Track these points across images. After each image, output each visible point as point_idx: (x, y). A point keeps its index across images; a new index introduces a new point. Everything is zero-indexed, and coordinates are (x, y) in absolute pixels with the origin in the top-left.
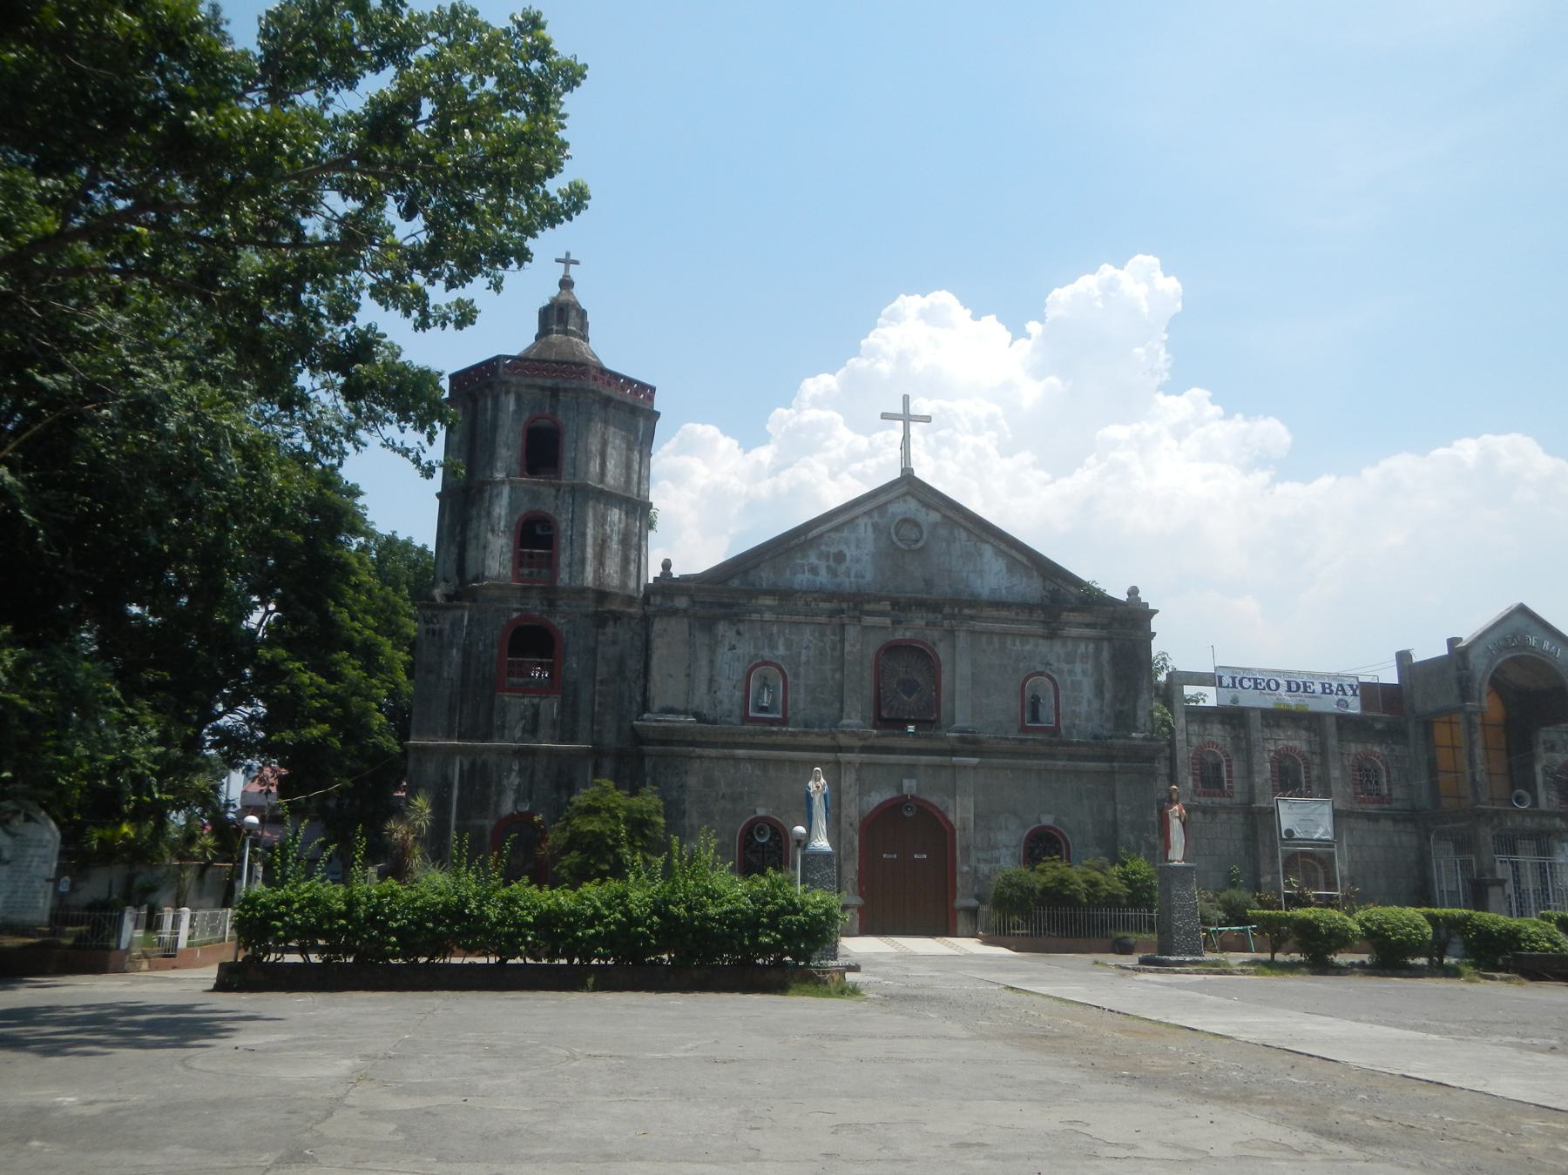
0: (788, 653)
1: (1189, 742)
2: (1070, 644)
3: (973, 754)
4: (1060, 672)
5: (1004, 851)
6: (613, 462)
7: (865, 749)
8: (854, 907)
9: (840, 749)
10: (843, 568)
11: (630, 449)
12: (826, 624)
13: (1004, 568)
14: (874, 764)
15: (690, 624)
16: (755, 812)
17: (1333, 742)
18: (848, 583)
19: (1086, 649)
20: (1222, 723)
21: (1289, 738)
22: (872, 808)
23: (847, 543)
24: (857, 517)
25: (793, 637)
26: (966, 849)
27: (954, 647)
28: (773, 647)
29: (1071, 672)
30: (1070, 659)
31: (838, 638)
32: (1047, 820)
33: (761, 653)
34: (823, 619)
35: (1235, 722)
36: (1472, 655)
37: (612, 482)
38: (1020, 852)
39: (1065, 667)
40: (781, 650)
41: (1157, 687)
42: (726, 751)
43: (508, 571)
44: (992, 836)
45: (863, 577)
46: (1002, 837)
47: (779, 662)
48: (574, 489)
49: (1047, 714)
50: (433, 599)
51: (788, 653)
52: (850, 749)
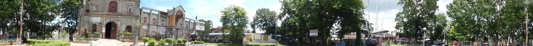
3: (121, 15)
7: (106, 15)
9: (104, 15)
41: (140, 9)
46: (123, 26)
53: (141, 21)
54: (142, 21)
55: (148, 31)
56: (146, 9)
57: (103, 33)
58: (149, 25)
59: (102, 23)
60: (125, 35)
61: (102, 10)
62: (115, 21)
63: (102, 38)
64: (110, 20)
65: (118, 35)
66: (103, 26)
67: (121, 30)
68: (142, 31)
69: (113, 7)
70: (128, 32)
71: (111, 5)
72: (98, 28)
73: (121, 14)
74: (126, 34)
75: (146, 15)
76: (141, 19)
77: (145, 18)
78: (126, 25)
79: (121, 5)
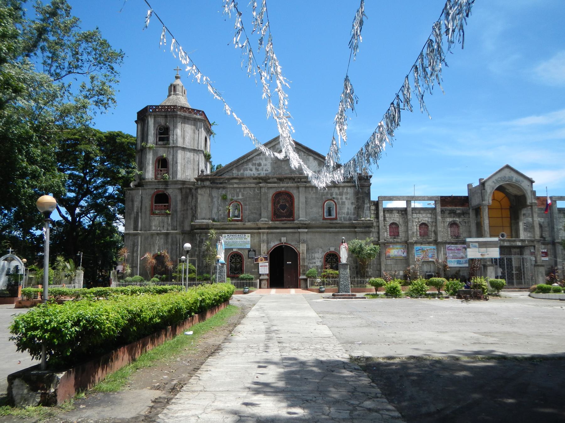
1: (385, 220)
2: (341, 189)
4: (337, 199)
5: (317, 260)
8: (265, 280)
9: (260, 228)
10: (260, 168)
11: (194, 133)
13: (317, 165)
14: (272, 233)
17: (439, 218)
18: (263, 174)
19: (347, 190)
20: (398, 213)
21: (424, 217)
22: (271, 247)
26: (304, 259)
27: (299, 192)
28: (238, 196)
29: (341, 199)
30: (341, 194)
32: (332, 249)
34: (253, 185)
35: (403, 213)
36: (487, 185)
37: (188, 144)
38: (323, 260)
39: (339, 197)
40: (240, 197)
41: (374, 202)
43: (154, 177)
44: (313, 255)
45: (268, 171)
46: (317, 255)
47: (239, 201)
48: (173, 147)
49: (334, 213)
50: (130, 187)
52: (264, 228)
53: (381, 237)
54: (386, 235)
55: (406, 261)
56: (391, 199)
57: (260, 275)
58: (408, 245)
59: (256, 249)
60: (324, 276)
61: (255, 216)
62: (293, 244)
63: (260, 287)
64: (279, 242)
65: (305, 277)
66: (260, 257)
67: (311, 266)
68: (389, 262)
69: (283, 207)
70: (332, 268)
71: (279, 202)
72: (247, 263)
73: (305, 224)
74: (325, 273)
75: (396, 218)
76: (379, 229)
77: (394, 226)
78: (323, 251)
79: (302, 199)
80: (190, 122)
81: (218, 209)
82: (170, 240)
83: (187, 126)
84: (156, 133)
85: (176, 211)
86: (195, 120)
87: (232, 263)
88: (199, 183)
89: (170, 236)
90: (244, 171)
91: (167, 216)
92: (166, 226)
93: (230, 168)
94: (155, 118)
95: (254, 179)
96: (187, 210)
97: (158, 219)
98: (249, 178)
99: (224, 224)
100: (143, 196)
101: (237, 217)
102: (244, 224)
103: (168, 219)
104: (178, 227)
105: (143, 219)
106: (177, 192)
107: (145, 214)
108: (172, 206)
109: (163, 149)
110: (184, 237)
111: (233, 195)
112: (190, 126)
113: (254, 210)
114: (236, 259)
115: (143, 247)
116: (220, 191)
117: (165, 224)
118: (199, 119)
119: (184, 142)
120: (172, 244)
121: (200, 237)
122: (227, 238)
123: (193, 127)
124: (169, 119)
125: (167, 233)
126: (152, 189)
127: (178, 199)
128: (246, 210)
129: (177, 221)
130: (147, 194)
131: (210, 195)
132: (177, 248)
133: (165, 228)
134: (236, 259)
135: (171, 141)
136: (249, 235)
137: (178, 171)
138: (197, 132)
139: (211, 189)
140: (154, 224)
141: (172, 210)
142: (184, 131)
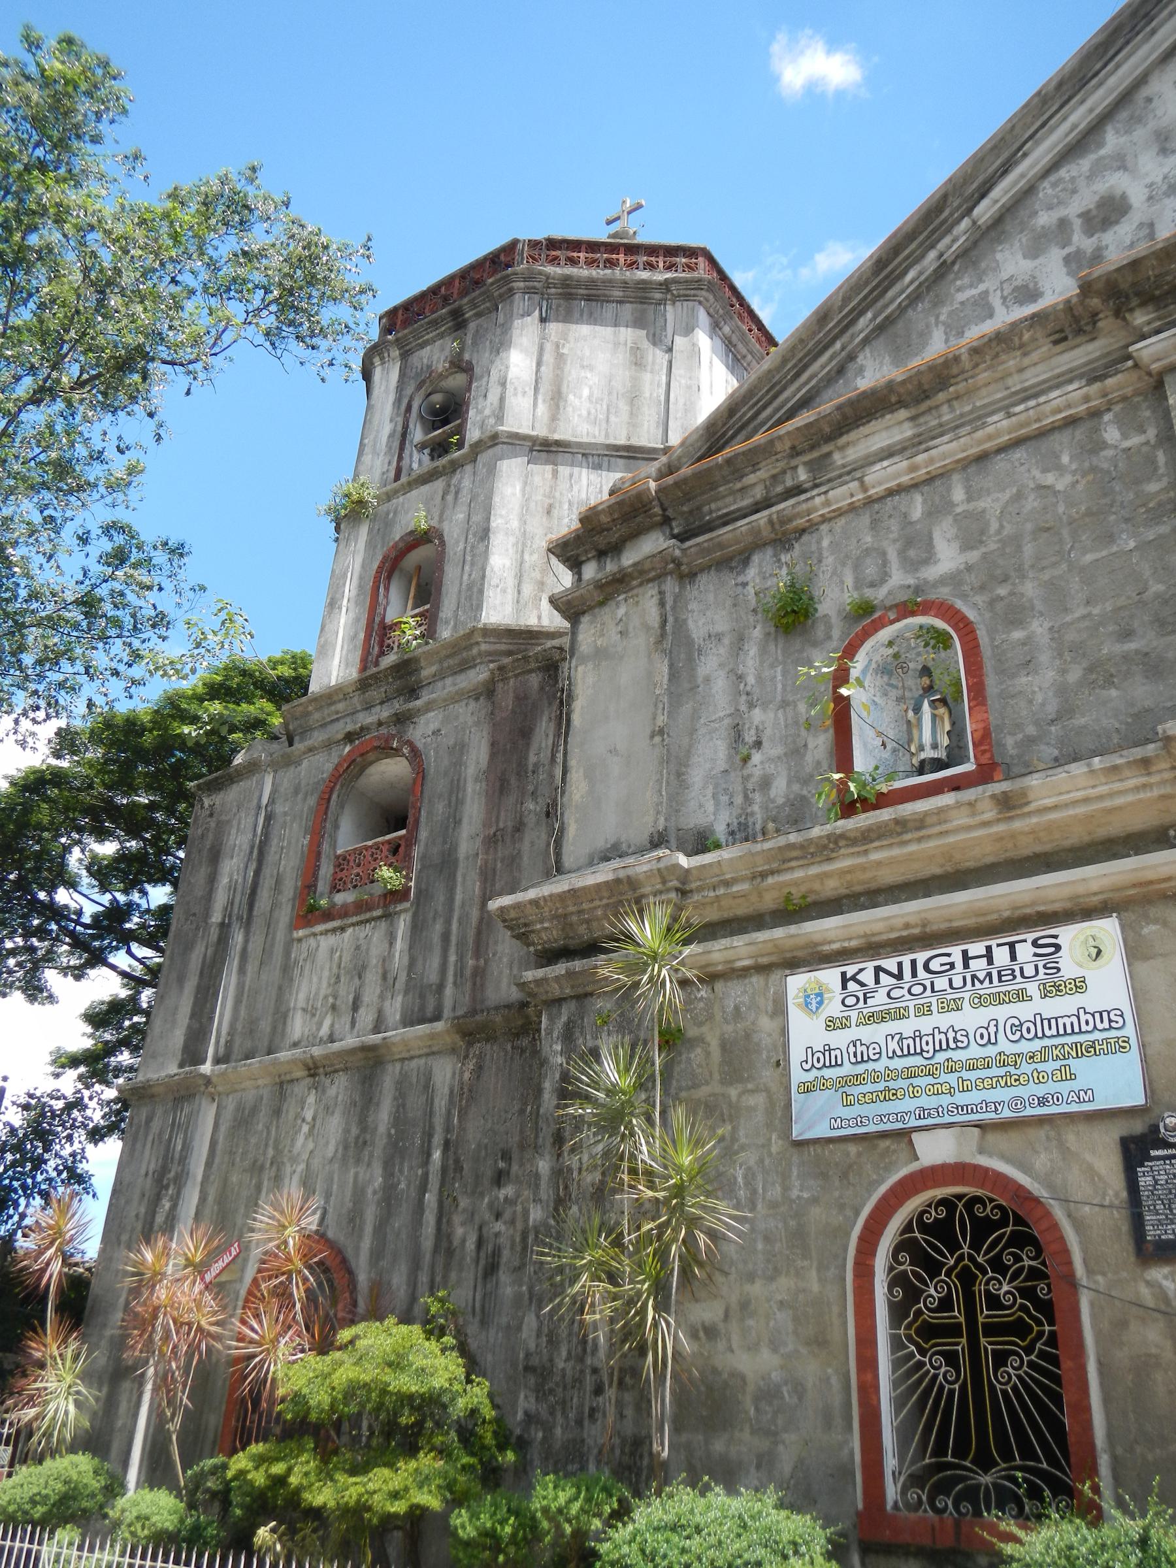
0: (974, 556)
6: (586, 392)
11: (637, 361)
12: (1095, 414)
15: (661, 593)
16: (917, 1159)
23: (1121, 162)
24: (1142, 80)
25: (982, 504)
31: (1151, 433)
33: (879, 595)
42: (779, 933)
47: (944, 593)
51: (974, 556)
80: (609, 310)
81: (737, 733)
82: (383, 1116)
83: (584, 329)
84: (399, 428)
85: (447, 864)
86: (641, 294)
87: (929, 1332)
88: (590, 571)
89: (388, 1081)
90: (956, 328)
91: (388, 916)
92: (371, 992)
93: (821, 366)
94: (405, 355)
95: (1060, 339)
96: (519, 827)
97: (332, 951)
98: (1003, 340)
99: (785, 858)
100: (279, 809)
101: (939, 765)
102: (1007, 804)
103: (391, 939)
104: (449, 991)
105: (251, 968)
106: (468, 714)
107: (269, 925)
108: (423, 834)
109: (425, 489)
110: (479, 1069)
111: (871, 570)
112: (606, 332)
113: (1127, 634)
114: (967, 1279)
115: (211, 1199)
116: (752, 573)
117: (372, 977)
118: (666, 285)
119: (554, 418)
120: (396, 1151)
121: (568, 1036)
122: (833, 1008)
123: (628, 334)
124: (472, 326)
125: (365, 1048)
126: (328, 745)
127: (471, 771)
128: (1028, 664)
129: (446, 937)
130: (297, 791)
131: (663, 635)
132: (423, 1188)
133: (366, 1017)
134: (967, 1279)
135: (473, 434)
136: (1108, 929)
137: (492, 578)
138: (661, 357)
139: (670, 586)
140: (302, 996)
141: (423, 858)
142: (560, 358)
